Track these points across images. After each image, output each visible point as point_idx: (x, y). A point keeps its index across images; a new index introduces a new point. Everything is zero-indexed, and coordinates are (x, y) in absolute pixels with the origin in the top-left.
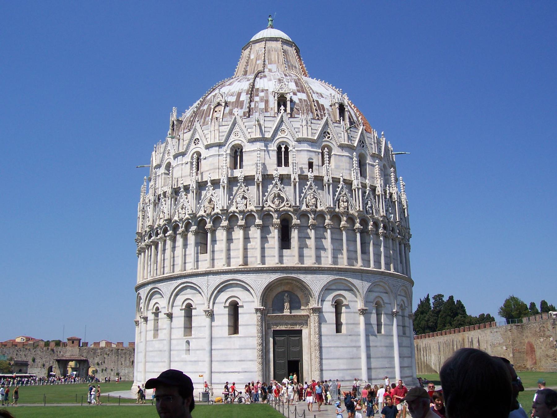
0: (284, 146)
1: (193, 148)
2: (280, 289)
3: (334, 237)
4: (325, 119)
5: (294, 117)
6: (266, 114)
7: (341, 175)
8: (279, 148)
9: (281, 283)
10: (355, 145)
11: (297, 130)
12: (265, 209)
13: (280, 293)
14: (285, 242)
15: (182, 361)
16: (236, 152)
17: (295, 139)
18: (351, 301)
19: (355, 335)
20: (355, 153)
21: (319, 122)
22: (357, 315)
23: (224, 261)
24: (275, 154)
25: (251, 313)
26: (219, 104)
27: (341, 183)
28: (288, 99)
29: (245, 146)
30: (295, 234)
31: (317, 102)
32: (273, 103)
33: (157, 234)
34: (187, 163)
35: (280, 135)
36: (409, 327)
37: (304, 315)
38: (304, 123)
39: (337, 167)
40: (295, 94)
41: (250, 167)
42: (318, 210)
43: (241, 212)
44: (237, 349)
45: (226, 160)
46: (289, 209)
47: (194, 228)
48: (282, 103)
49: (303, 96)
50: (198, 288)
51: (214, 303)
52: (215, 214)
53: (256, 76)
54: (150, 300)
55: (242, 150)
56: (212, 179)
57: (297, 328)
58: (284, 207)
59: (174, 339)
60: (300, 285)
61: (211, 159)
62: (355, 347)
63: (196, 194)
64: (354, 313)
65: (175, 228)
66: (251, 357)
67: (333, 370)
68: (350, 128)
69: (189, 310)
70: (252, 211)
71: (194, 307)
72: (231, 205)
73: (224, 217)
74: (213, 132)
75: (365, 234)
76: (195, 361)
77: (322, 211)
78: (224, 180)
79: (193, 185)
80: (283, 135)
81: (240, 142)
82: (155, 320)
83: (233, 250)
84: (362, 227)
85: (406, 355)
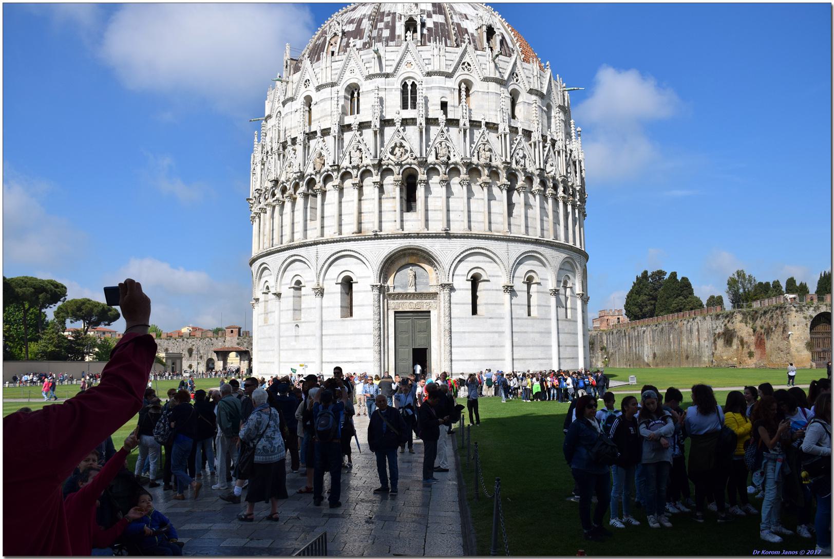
1: (303, 92)
4: (464, 45)
6: (391, 43)
8: (405, 86)
10: (506, 77)
11: (427, 62)
12: (383, 162)
14: (409, 202)
23: (335, 228)
28: (419, 22)
30: (420, 191)
31: (458, 25)
32: (400, 28)
38: (436, 51)
40: (429, 16)
41: (367, 112)
43: (354, 167)
49: (439, 19)
54: (260, 278)
58: (408, 159)
61: (322, 104)
77: (456, 164)
78: (335, 129)
79: (301, 137)
80: (409, 70)
81: (355, 81)
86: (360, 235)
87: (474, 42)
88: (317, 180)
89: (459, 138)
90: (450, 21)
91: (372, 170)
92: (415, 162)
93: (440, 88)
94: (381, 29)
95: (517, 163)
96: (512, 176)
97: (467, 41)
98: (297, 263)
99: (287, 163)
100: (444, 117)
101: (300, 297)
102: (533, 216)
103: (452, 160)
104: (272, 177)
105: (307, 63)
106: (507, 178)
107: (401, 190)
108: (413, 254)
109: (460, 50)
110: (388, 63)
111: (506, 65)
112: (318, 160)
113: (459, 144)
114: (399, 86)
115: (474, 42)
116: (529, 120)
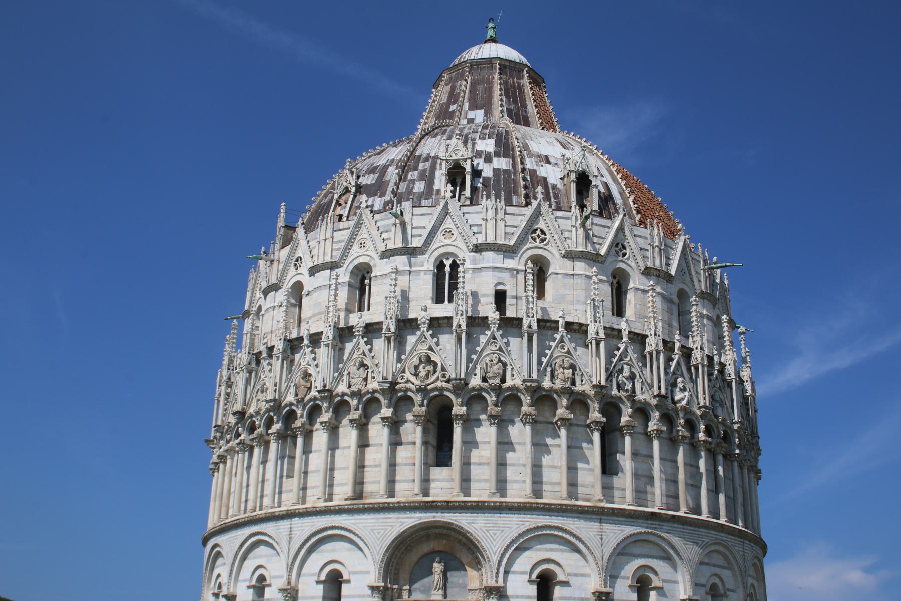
2: (426, 548)
4: (535, 203)
6: (424, 202)
7: (561, 313)
8: (440, 266)
10: (602, 252)
11: (475, 229)
12: (398, 387)
13: (426, 555)
14: (440, 451)
16: (364, 279)
17: (471, 247)
18: (576, 575)
25: (363, 596)
27: (560, 329)
28: (468, 168)
29: (375, 266)
31: (533, 173)
34: (281, 306)
35: (440, 240)
38: (491, 214)
39: (561, 299)
42: (505, 385)
43: (353, 394)
46: (445, 385)
49: (502, 163)
50: (275, 544)
51: (299, 575)
52: (311, 400)
56: (312, 332)
58: (436, 382)
60: (463, 540)
70: (375, 391)
71: (268, 582)
72: (337, 380)
73: (325, 405)
74: (322, 243)
75: (618, 434)
77: (514, 388)
78: (329, 334)
79: (279, 345)
80: (448, 242)
83: (340, 469)
84: (604, 420)
86: (359, 504)
87: (556, 197)
88: (299, 412)
89: (521, 349)
90: (520, 167)
91: (381, 398)
92: (449, 386)
93: (495, 269)
94: (413, 181)
95: (619, 387)
96: (611, 408)
97: (540, 196)
99: (258, 387)
100: (497, 315)
102: (653, 477)
103: (509, 382)
104: (238, 407)
105: (301, 231)
106: (602, 411)
107: (425, 431)
108: (441, 536)
109: (529, 211)
110: (415, 232)
111: (606, 232)
112: (303, 382)
113: (521, 357)
115: (556, 197)
116: (644, 317)
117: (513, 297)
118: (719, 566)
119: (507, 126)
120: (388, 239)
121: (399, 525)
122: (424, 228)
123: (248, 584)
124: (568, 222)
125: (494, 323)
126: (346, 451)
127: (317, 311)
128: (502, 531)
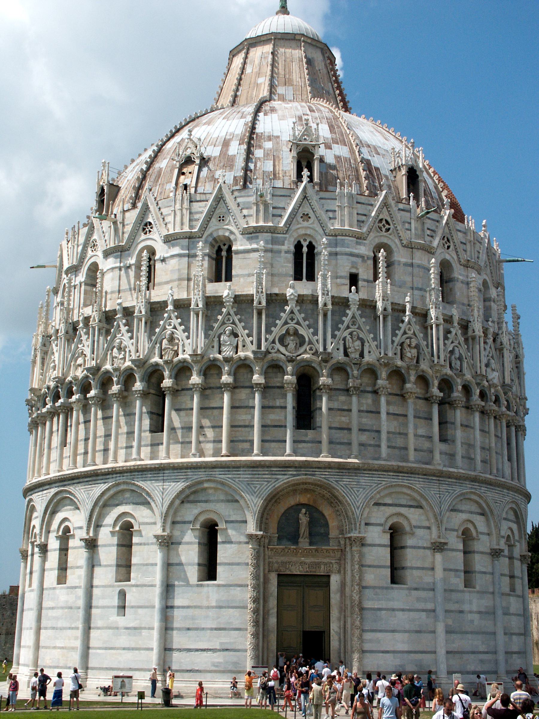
0: (307, 243)
2: (292, 501)
3: (391, 411)
5: (327, 191)
8: (298, 246)
9: (295, 490)
15: (110, 628)
16: (219, 250)
18: (419, 527)
19: (424, 589)
20: (433, 260)
21: (371, 200)
22: (428, 552)
24: (291, 257)
26: (189, 161)
27: (407, 313)
29: (236, 240)
33: (70, 393)
36: (522, 578)
37: (333, 550)
44: (213, 607)
45: (202, 266)
47: (138, 386)
48: (304, 164)
52: (180, 361)
53: (258, 110)
54: (54, 513)
55: (230, 247)
57: (322, 571)
59: (97, 587)
60: (328, 495)
62: (423, 610)
63: (146, 323)
64: (424, 548)
65: (106, 382)
66: (236, 623)
67: (383, 652)
68: (428, 213)
69: (126, 532)
71: (136, 527)
74: (178, 213)
76: (135, 628)
78: (197, 301)
81: (227, 234)
82: (61, 550)
84: (441, 394)
85: (517, 631)
96: (446, 384)
98: (127, 495)
101: (129, 546)
103: (367, 358)
108: (306, 491)
114: (289, 246)
117: (364, 280)
118: (511, 521)
119: (332, 112)
120: (248, 216)
121: (273, 480)
122: (284, 208)
123: (111, 529)
124: (408, 214)
125: (354, 304)
126: (216, 412)
127: (176, 276)
128: (364, 489)
